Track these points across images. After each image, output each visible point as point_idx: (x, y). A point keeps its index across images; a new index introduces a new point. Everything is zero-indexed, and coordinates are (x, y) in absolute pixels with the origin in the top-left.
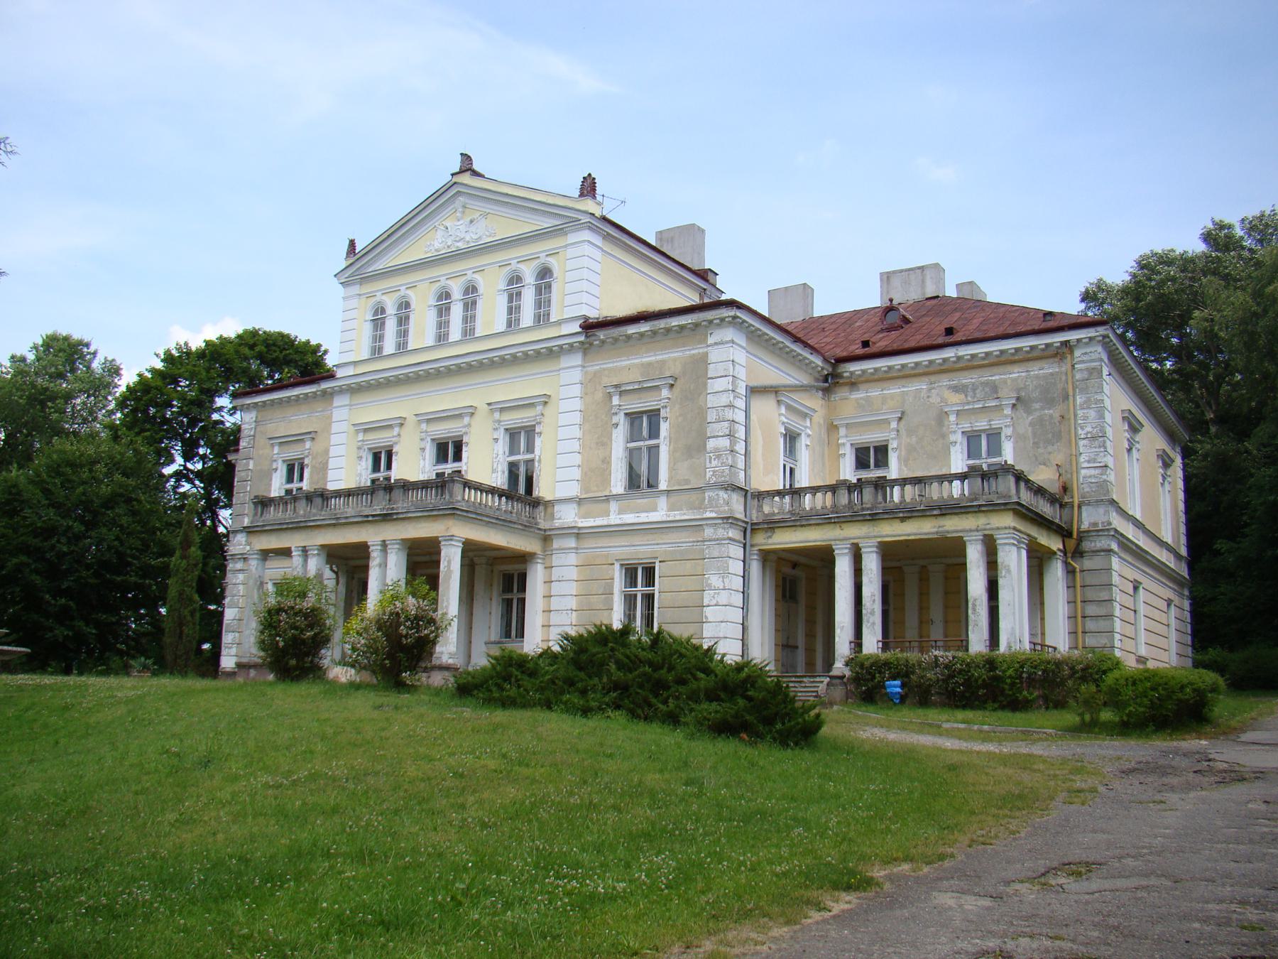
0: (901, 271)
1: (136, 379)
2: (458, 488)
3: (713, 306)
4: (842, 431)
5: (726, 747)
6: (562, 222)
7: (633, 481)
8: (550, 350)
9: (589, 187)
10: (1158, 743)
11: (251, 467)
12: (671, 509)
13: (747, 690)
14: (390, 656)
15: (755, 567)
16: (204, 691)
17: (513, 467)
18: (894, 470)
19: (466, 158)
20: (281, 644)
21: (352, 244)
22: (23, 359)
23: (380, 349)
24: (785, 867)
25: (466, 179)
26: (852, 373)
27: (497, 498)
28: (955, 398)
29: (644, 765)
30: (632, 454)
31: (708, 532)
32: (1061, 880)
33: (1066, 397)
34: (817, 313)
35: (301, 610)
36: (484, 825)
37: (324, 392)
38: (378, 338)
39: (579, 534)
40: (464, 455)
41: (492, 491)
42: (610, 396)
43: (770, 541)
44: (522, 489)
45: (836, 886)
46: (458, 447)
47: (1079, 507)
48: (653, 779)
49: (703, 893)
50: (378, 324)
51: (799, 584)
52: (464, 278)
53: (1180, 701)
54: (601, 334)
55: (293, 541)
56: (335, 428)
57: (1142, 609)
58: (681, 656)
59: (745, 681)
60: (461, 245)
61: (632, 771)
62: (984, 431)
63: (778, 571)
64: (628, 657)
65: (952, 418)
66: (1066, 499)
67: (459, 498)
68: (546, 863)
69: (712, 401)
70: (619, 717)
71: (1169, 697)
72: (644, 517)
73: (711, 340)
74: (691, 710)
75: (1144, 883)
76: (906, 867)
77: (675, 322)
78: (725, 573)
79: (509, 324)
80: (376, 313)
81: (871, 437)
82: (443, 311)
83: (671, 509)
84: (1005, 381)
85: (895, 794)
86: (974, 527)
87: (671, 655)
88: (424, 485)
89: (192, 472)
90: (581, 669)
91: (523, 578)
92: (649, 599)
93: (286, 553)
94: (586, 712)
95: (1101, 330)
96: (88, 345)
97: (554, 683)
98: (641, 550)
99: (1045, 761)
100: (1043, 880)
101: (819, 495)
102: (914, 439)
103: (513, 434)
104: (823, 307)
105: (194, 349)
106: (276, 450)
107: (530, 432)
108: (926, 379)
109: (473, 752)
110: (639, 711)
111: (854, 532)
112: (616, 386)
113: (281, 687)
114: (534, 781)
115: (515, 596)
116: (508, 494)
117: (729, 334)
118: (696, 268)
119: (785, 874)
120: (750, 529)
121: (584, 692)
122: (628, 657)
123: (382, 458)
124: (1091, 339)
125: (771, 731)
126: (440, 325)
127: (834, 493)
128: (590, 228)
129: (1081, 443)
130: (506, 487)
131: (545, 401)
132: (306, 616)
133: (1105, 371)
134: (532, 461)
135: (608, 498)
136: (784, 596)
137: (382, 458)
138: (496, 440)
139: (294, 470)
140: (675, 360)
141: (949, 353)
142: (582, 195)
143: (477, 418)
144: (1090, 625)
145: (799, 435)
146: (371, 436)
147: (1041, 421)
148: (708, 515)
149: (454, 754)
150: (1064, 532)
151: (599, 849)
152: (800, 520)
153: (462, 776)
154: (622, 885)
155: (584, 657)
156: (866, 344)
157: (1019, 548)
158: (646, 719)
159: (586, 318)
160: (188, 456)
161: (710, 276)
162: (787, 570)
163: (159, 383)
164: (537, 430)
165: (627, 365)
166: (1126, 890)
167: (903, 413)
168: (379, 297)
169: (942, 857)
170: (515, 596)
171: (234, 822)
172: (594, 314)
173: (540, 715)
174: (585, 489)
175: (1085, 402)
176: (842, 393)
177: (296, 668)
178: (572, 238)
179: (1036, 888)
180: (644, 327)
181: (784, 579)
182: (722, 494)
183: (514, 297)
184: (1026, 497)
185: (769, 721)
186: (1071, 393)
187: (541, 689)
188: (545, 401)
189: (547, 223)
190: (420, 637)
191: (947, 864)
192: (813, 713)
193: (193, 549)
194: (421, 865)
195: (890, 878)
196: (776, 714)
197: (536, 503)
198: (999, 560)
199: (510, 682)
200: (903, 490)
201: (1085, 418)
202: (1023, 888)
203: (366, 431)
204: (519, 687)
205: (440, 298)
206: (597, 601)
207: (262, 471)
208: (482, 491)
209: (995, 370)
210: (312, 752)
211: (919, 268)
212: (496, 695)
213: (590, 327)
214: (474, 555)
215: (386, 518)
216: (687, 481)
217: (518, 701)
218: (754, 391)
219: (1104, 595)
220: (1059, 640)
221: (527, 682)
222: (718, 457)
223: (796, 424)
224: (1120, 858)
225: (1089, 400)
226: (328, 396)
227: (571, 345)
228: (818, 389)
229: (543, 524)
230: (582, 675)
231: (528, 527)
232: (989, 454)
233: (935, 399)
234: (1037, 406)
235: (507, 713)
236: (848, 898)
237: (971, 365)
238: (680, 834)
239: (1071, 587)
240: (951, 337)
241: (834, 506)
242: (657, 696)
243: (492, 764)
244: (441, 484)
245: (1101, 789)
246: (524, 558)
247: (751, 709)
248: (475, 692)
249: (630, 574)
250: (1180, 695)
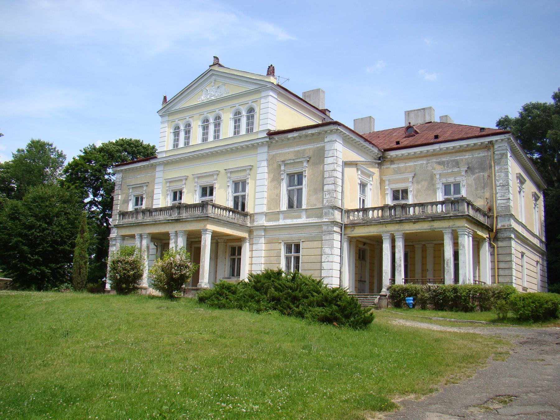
0: (414, 111)
1: (72, 160)
2: (210, 207)
3: (327, 124)
4: (387, 183)
5: (326, 328)
6: (260, 87)
7: (291, 206)
8: (253, 145)
9: (271, 71)
10: (535, 328)
11: (120, 198)
12: (307, 217)
13: (337, 301)
14: (168, 283)
15: (345, 245)
16: (82, 299)
17: (236, 199)
18: (411, 200)
19: (216, 58)
20: (119, 277)
21: (165, 98)
22: (23, 151)
23: (177, 145)
24: (348, 396)
25: (216, 68)
26: (391, 156)
27: (228, 213)
28: (438, 169)
29: (283, 338)
30: (290, 193)
31: (325, 228)
32: (496, 406)
33: (490, 167)
34: (375, 131)
35: (128, 262)
36: (195, 370)
37: (152, 165)
38: (176, 140)
39: (265, 229)
40: (214, 193)
41: (226, 209)
42: (280, 166)
43: (353, 232)
44: (240, 209)
45: (374, 409)
46: (212, 190)
47: (496, 218)
48: (286, 346)
49: (301, 411)
50: (176, 134)
51: (366, 254)
52: (214, 113)
53: (546, 308)
54: (276, 137)
55: (136, 231)
56: (157, 181)
57: (525, 265)
58: (306, 284)
59: (336, 297)
60: (213, 98)
61: (276, 341)
62: (452, 183)
63: (357, 246)
64: (280, 285)
65: (438, 176)
66: (490, 214)
67: (210, 212)
68: (221, 393)
69: (326, 168)
70: (276, 314)
71: (541, 307)
72: (295, 221)
73: (326, 140)
74: (310, 311)
75: (542, 410)
76: (412, 396)
77: (310, 132)
78: (332, 247)
79: (235, 133)
80: (175, 129)
81: (400, 186)
82: (205, 128)
83: (307, 217)
84: (462, 160)
85: (408, 354)
86: (447, 226)
87: (301, 284)
88: (195, 206)
89: (97, 201)
90: (257, 290)
91: (240, 249)
92: (297, 259)
93: (133, 237)
94: (258, 311)
95: (507, 136)
96: (51, 145)
97: (244, 297)
98: (293, 237)
99: (482, 337)
100: (486, 405)
101: (376, 211)
102: (420, 186)
103: (236, 184)
104: (379, 127)
105: (98, 147)
106: (131, 191)
107: (244, 183)
108: (425, 159)
109: (198, 331)
110: (285, 311)
111: (392, 228)
112: (283, 161)
113: (118, 297)
114: (226, 346)
115: (236, 257)
116: (234, 211)
117: (334, 137)
118: (320, 108)
119: (346, 401)
120: (344, 227)
121: (258, 302)
122: (280, 285)
123: (177, 195)
124: (502, 140)
125: (348, 321)
126: (204, 134)
127: (382, 210)
128: (271, 90)
129: (498, 188)
130: (233, 207)
131: (251, 168)
132: (130, 264)
133: (509, 155)
134: (245, 195)
135: (279, 213)
136: (359, 258)
137: (177, 195)
138: (228, 186)
139: (138, 200)
140: (310, 149)
141: (436, 147)
142: (268, 74)
143: (220, 176)
144: (501, 272)
145: (367, 184)
146: (172, 184)
147: (479, 177)
148: (324, 220)
149: (190, 331)
150: (489, 229)
151: (248, 384)
152: (367, 223)
153: (190, 343)
154: (257, 407)
155: (259, 285)
156: (398, 143)
157: (469, 237)
158: (288, 315)
159: (269, 130)
160: (95, 195)
161: (327, 113)
162: (361, 246)
163: (83, 162)
164: (247, 182)
165: (288, 152)
166: (533, 414)
167: (415, 175)
168: (177, 122)
169: (431, 391)
170: (236, 257)
171: (68, 366)
172: (273, 129)
173: (236, 312)
174: (269, 208)
175: (499, 169)
176: (386, 166)
177: (126, 288)
178: (263, 94)
179: (482, 411)
180: (295, 134)
181: (359, 250)
182: (331, 210)
183: (237, 121)
184: (471, 213)
185: (347, 317)
186: (493, 165)
187: (238, 300)
188: (251, 168)
189: (252, 87)
190: (182, 275)
191: (434, 394)
192: (369, 313)
193: (85, 234)
194: (153, 392)
195: (403, 403)
196: (351, 313)
197: (246, 215)
198: (459, 242)
199: (222, 297)
200: (414, 209)
201: (500, 176)
202: (475, 410)
203: (170, 182)
204: (227, 298)
205: (204, 122)
206: (273, 260)
207: (123, 202)
208: (221, 209)
209: (458, 154)
210: (119, 329)
211: (423, 109)
212: (216, 302)
213: (271, 134)
214: (216, 238)
215: (177, 221)
216: (315, 205)
217: (226, 305)
218: (347, 164)
219: (508, 259)
220: (487, 279)
221: (231, 296)
222: (329, 194)
223: (365, 179)
224: (527, 393)
225: (501, 168)
226: (154, 167)
227: (262, 143)
228: (376, 163)
229: (249, 225)
230: (258, 293)
231: (241, 227)
232: (455, 193)
233: (429, 168)
234: (477, 171)
235: (220, 311)
236: (380, 416)
237: (447, 152)
238: (294, 377)
239: (492, 254)
240: (437, 140)
241: (382, 216)
242: (294, 304)
243: (207, 337)
244: (203, 205)
245: (511, 352)
246: (241, 240)
247: (340, 311)
248: (206, 301)
249: (289, 248)
250: (546, 306)
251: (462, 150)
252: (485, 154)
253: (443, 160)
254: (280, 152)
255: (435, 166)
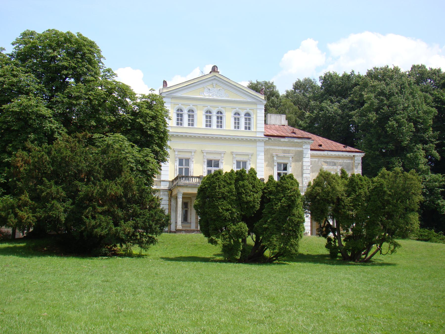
21: (165, 83)
84: (338, 162)
138: (234, 163)
140: (293, 150)
189: (249, 100)
222: (307, 179)
251: (339, 157)
252: (350, 161)
253: (328, 160)
254: (272, 148)
255: (323, 163)
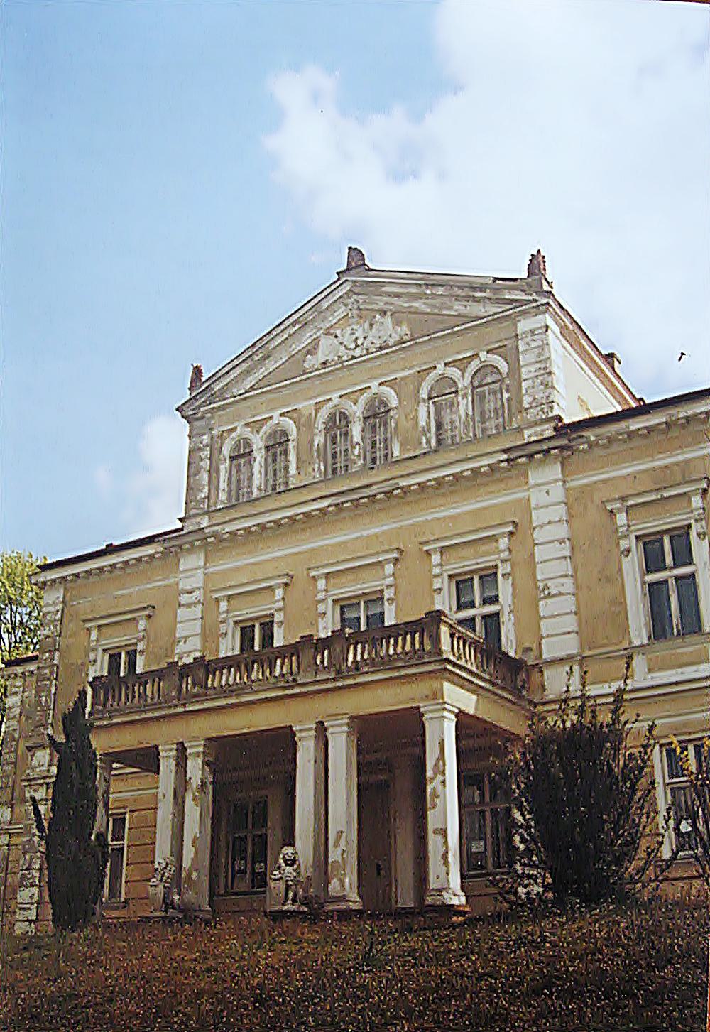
7: (659, 630)
30: (656, 592)
72: (690, 672)
112: (623, 499)
178: (523, 326)
